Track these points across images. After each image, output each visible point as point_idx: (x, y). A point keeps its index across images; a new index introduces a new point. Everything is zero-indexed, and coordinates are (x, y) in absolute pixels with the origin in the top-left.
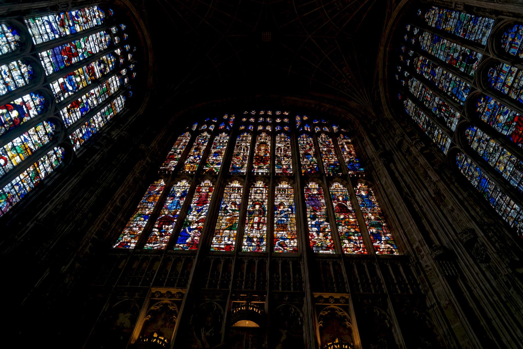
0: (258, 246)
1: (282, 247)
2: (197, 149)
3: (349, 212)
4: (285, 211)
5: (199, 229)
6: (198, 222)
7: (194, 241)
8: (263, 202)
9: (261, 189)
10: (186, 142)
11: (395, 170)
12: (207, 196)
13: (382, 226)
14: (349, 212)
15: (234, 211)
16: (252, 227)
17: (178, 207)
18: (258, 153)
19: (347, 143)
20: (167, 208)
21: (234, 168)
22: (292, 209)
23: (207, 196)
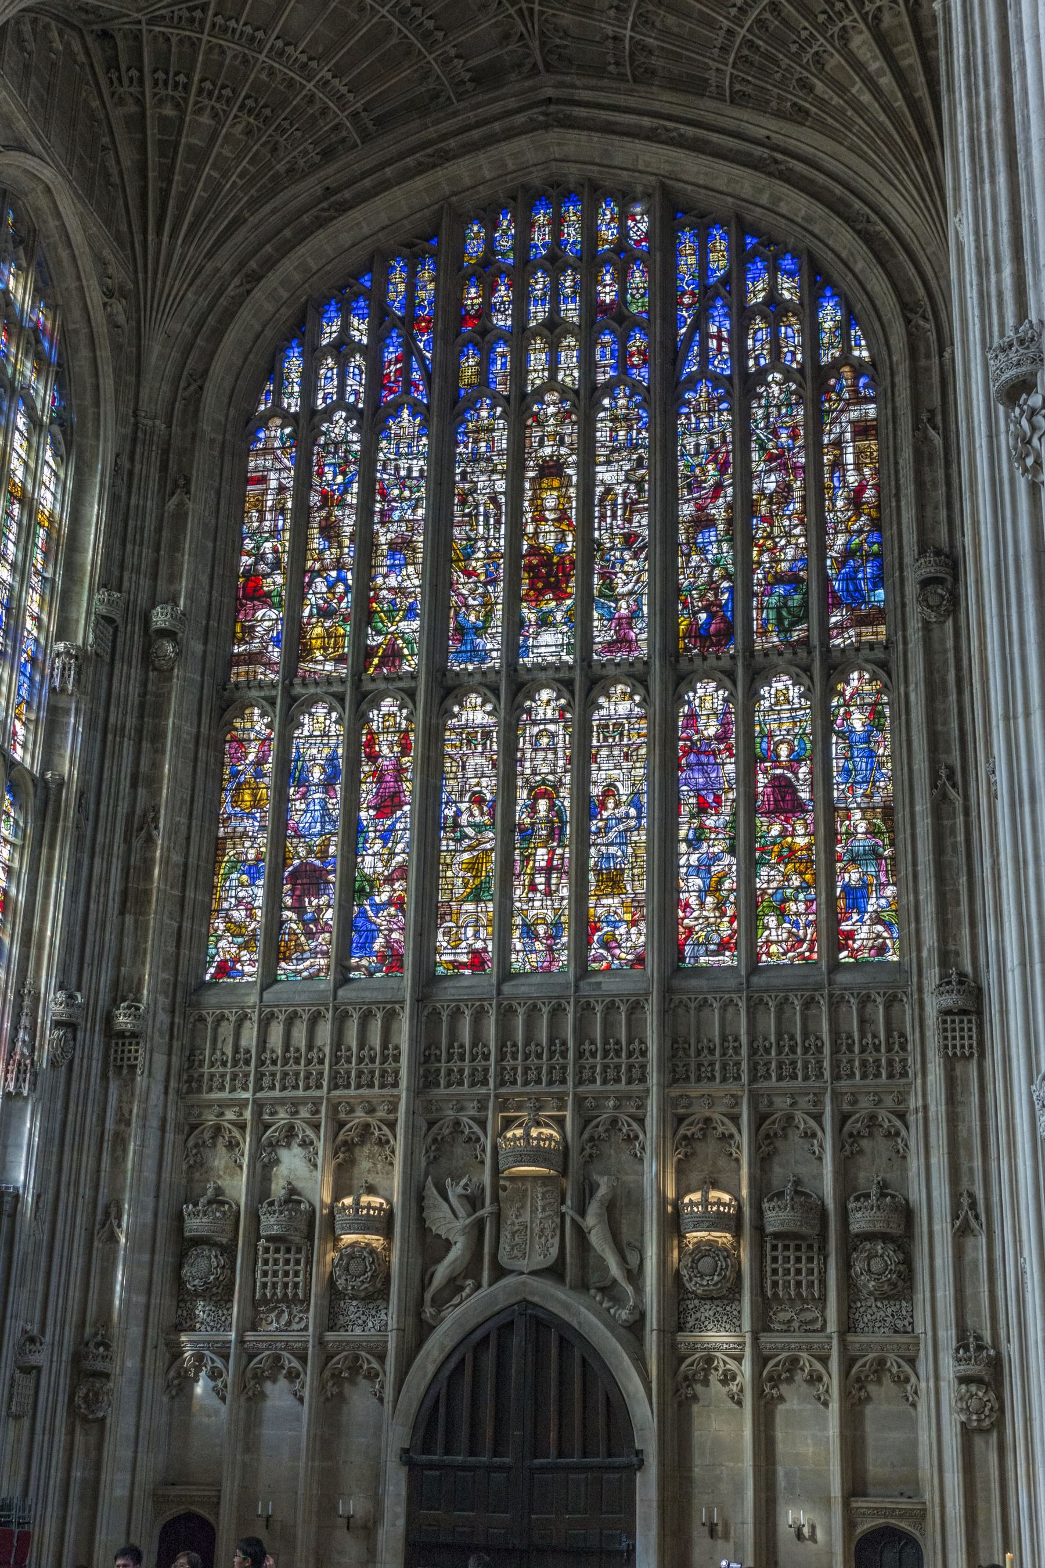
0: (550, 949)
1: (608, 949)
2: (330, 531)
3: (799, 807)
4: (620, 820)
5: (399, 903)
6: (389, 880)
7: (392, 948)
8: (557, 786)
9: (552, 727)
10: (281, 489)
11: (951, 655)
12: (400, 770)
13: (879, 857)
14: (799, 807)
15: (479, 827)
16: (533, 887)
17: (329, 827)
18: (536, 534)
20: (299, 836)
21: (461, 630)
22: (639, 810)
23: (400, 770)
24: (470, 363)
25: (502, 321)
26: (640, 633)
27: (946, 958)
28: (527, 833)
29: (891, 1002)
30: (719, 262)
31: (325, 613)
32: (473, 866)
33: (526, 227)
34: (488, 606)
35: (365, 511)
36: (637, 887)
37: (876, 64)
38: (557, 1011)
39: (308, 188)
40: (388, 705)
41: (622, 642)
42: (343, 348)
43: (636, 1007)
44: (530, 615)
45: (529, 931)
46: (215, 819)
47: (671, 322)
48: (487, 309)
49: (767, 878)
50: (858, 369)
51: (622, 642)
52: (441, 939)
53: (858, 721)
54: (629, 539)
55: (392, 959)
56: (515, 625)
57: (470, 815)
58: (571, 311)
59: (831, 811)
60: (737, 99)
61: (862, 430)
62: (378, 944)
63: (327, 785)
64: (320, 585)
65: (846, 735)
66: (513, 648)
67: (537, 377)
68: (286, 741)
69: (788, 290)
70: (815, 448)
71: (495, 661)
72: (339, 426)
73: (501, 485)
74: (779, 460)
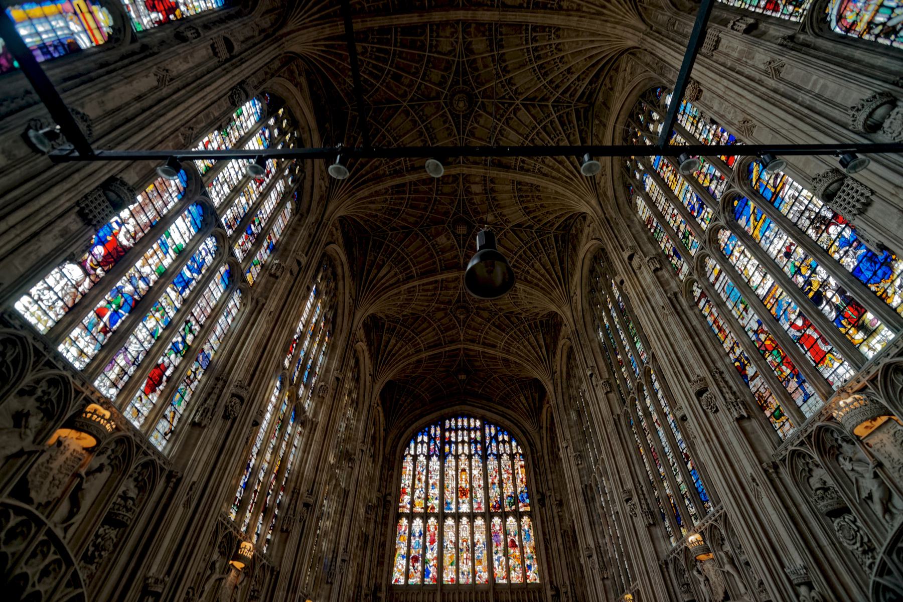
2: (419, 480)
3: (516, 546)
14: (516, 546)
19: (522, 467)
24: (447, 447)
25: (453, 439)
26: (483, 506)
27: (551, 583)
28: (462, 550)
29: (540, 592)
30: (493, 432)
31: (419, 498)
32: (451, 557)
33: (457, 422)
34: (452, 498)
35: (427, 476)
36: (485, 563)
37: (524, 401)
38: (471, 593)
39: (418, 412)
40: (432, 519)
41: (479, 508)
42: (422, 442)
43: (487, 593)
44: (460, 501)
45: (463, 573)
46: (395, 544)
47: (485, 443)
48: (450, 437)
49: (511, 562)
50: (520, 454)
51: (479, 508)
52: (444, 575)
53: (526, 528)
54: (479, 486)
55: (434, 579)
56: (458, 503)
57: (450, 546)
58: (466, 439)
59: (522, 548)
60: (498, 404)
61: (522, 467)
62: (431, 576)
63: (420, 536)
64: (418, 491)
65: (524, 530)
66: (458, 508)
67: (460, 452)
68: (410, 527)
69: (506, 438)
70: (513, 469)
71: (454, 511)
72: (422, 458)
73: (454, 473)
74: (507, 471)
